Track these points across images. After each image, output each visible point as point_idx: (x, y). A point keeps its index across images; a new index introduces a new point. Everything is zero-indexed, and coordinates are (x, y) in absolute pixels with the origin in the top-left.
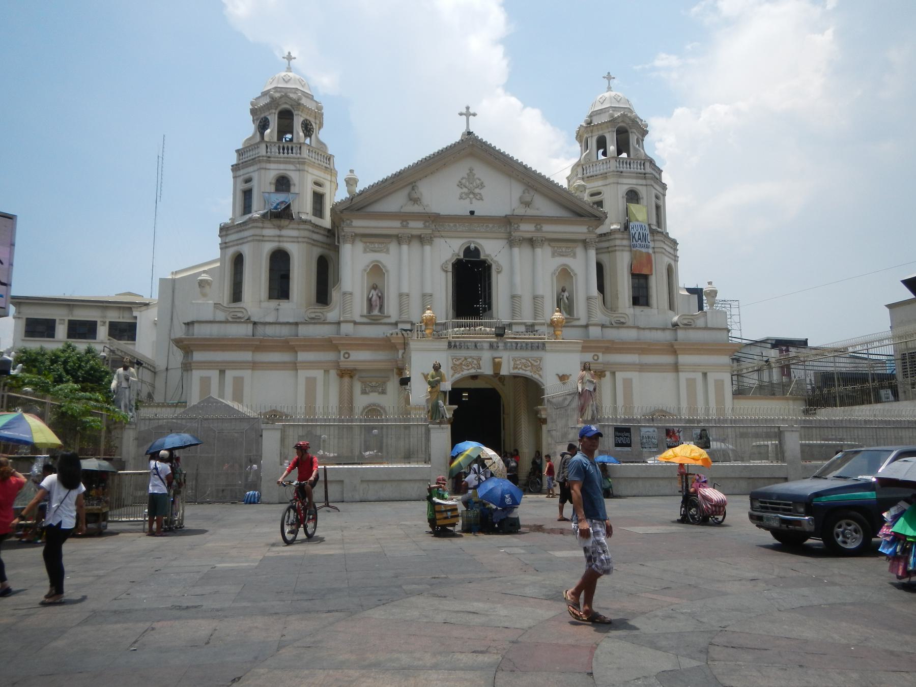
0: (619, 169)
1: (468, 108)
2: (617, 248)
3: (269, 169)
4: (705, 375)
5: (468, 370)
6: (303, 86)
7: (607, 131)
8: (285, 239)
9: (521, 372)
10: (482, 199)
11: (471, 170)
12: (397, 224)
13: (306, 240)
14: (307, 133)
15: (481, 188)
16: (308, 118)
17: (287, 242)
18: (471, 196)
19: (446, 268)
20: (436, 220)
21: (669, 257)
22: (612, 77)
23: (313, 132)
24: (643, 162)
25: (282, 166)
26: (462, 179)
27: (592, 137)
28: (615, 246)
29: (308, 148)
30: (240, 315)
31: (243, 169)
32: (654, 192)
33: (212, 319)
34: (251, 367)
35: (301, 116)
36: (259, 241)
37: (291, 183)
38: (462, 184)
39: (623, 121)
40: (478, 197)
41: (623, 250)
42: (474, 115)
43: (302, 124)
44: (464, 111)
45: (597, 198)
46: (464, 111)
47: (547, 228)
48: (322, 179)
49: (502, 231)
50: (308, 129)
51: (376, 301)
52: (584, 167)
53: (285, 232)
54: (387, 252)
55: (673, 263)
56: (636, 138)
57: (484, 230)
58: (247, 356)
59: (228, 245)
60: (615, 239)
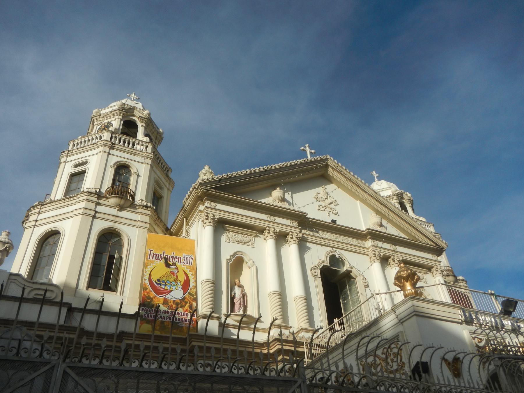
3: (112, 155)
8: (122, 220)
12: (264, 217)
16: (151, 135)
18: (328, 209)
19: (315, 272)
25: (126, 155)
29: (154, 150)
31: (77, 154)
36: (89, 215)
40: (334, 212)
47: (400, 249)
48: (162, 183)
49: (361, 246)
57: (344, 242)
59: (38, 223)
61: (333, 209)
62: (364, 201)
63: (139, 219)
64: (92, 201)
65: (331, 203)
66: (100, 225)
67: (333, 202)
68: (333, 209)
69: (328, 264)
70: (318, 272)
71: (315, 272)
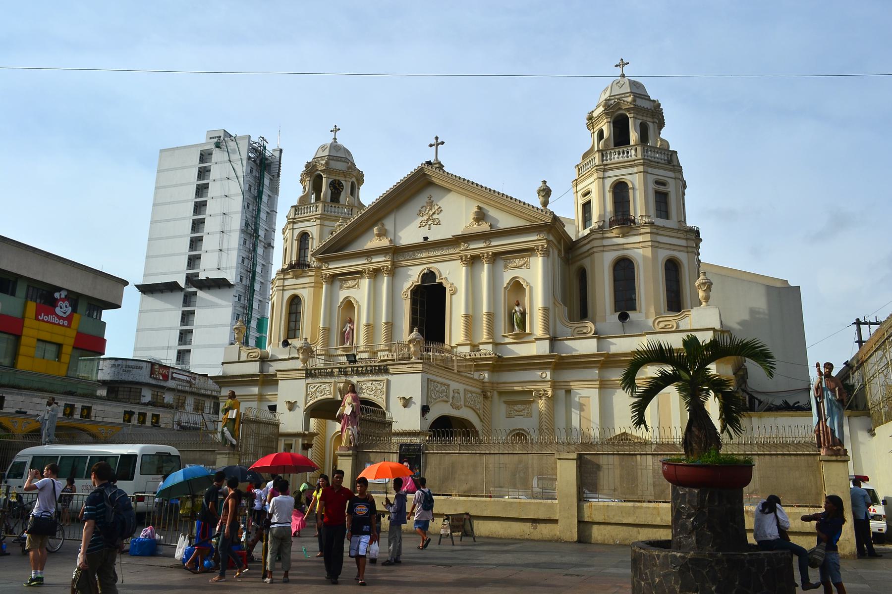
0: (605, 162)
1: (437, 138)
2: (595, 250)
3: (295, 229)
5: (321, 396)
6: (337, 152)
7: (603, 123)
13: (313, 285)
14: (336, 191)
15: (438, 214)
16: (337, 178)
17: (300, 288)
18: (430, 222)
19: (406, 295)
20: (397, 252)
21: (674, 250)
22: (626, 62)
23: (343, 189)
24: (634, 148)
26: (422, 208)
27: (594, 133)
28: (593, 247)
30: (254, 354)
33: (237, 360)
34: (256, 399)
35: (329, 178)
37: (311, 237)
38: (420, 213)
39: (620, 109)
41: (603, 251)
42: (443, 143)
43: (330, 184)
44: (433, 141)
45: (586, 199)
46: (433, 141)
49: (456, 252)
50: (336, 187)
51: (349, 333)
52: (579, 167)
53: (301, 281)
54: (359, 288)
55: (682, 257)
56: (639, 122)
57: (439, 254)
58: (255, 390)
60: (593, 239)
62: (467, 196)
63: (308, 282)
64: (281, 279)
65: (434, 213)
66: (288, 294)
67: (435, 212)
68: (435, 219)
69: (420, 283)
70: (409, 293)
71: (406, 295)
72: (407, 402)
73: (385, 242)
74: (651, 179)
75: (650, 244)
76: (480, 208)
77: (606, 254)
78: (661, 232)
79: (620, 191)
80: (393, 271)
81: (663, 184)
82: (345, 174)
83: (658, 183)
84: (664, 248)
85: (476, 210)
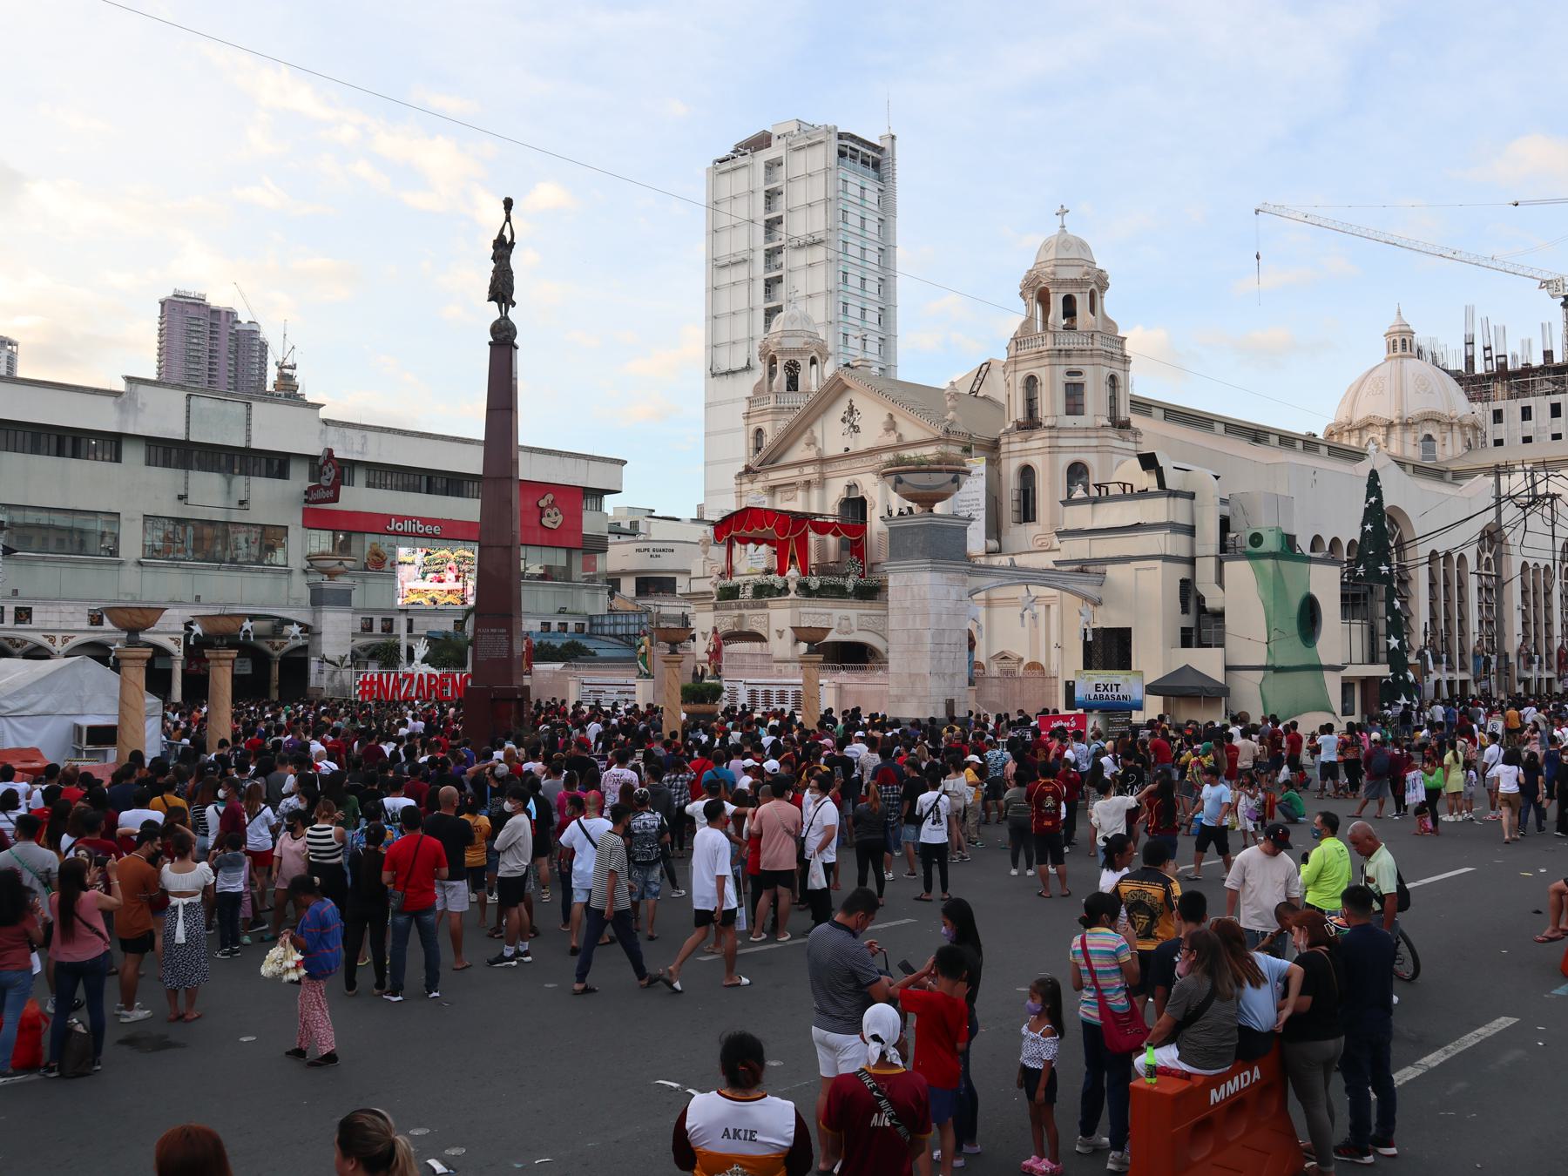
4: (1048, 607)
9: (754, 628)
10: (858, 431)
11: (851, 401)
12: (795, 472)
16: (792, 358)
20: (823, 461)
32: (1063, 369)
61: (854, 427)
72: (780, 633)
73: (811, 454)
74: (1061, 370)
75: (1048, 450)
76: (891, 416)
77: (1012, 461)
78: (1061, 435)
79: (1031, 381)
80: (822, 483)
81: (1079, 373)
82: (801, 351)
83: (1069, 373)
84: (1066, 452)
85: (885, 418)
